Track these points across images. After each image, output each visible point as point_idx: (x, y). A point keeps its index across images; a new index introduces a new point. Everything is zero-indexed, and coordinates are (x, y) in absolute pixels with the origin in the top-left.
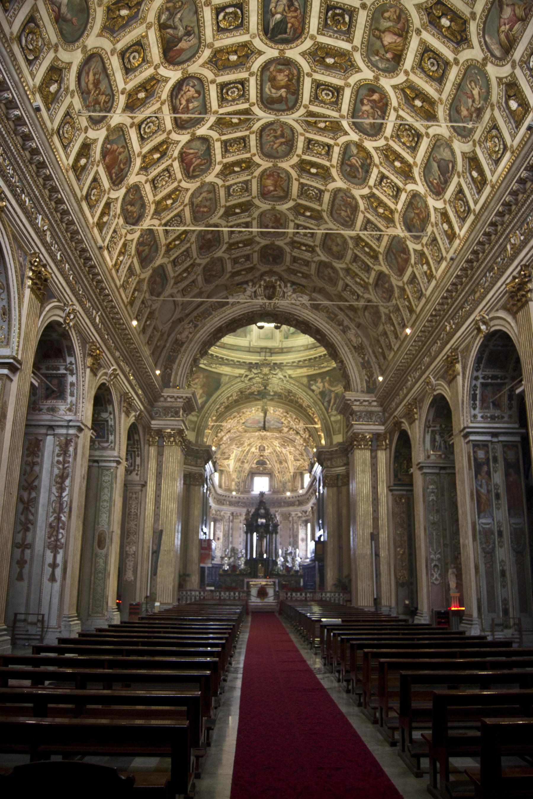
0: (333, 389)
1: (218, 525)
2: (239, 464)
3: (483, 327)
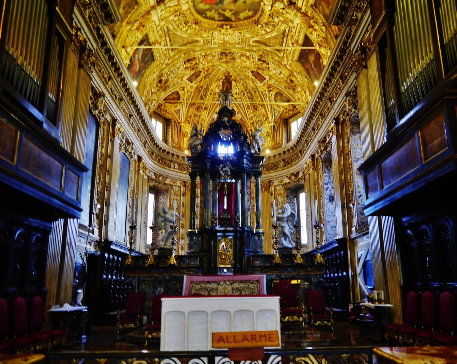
1: (162, 199)
2: (192, 111)
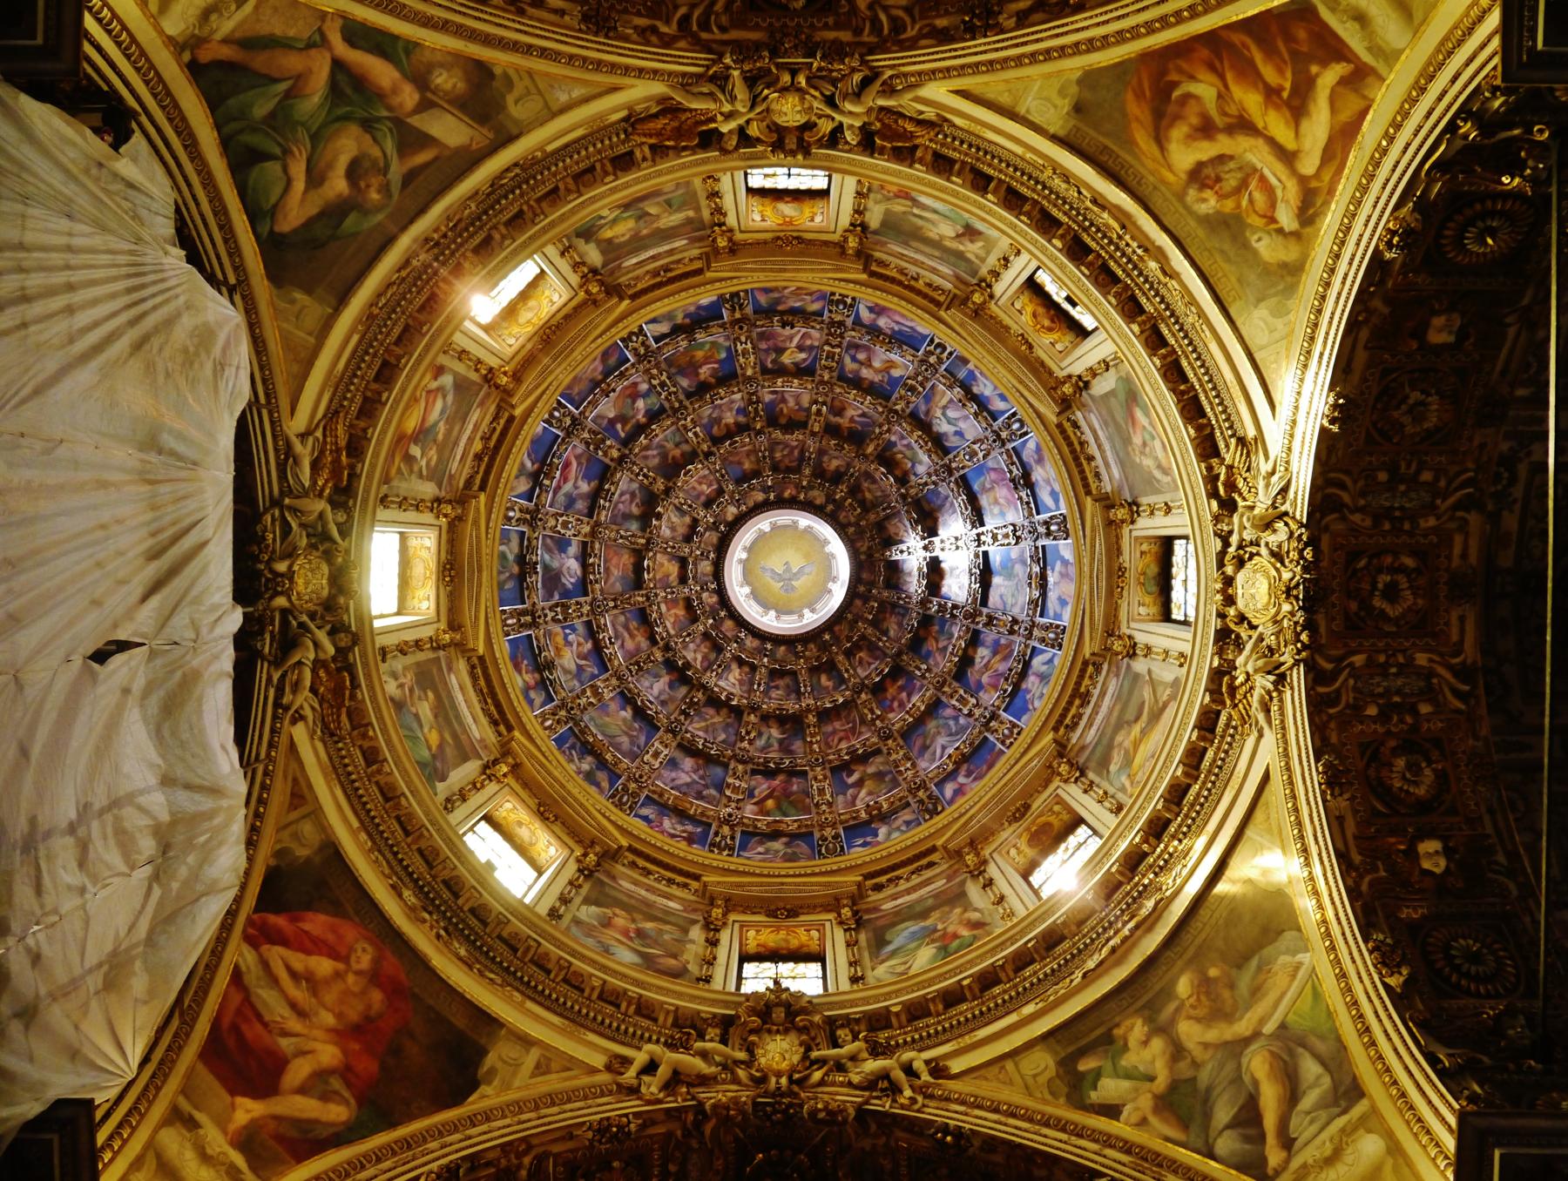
0: (1243, 1027)
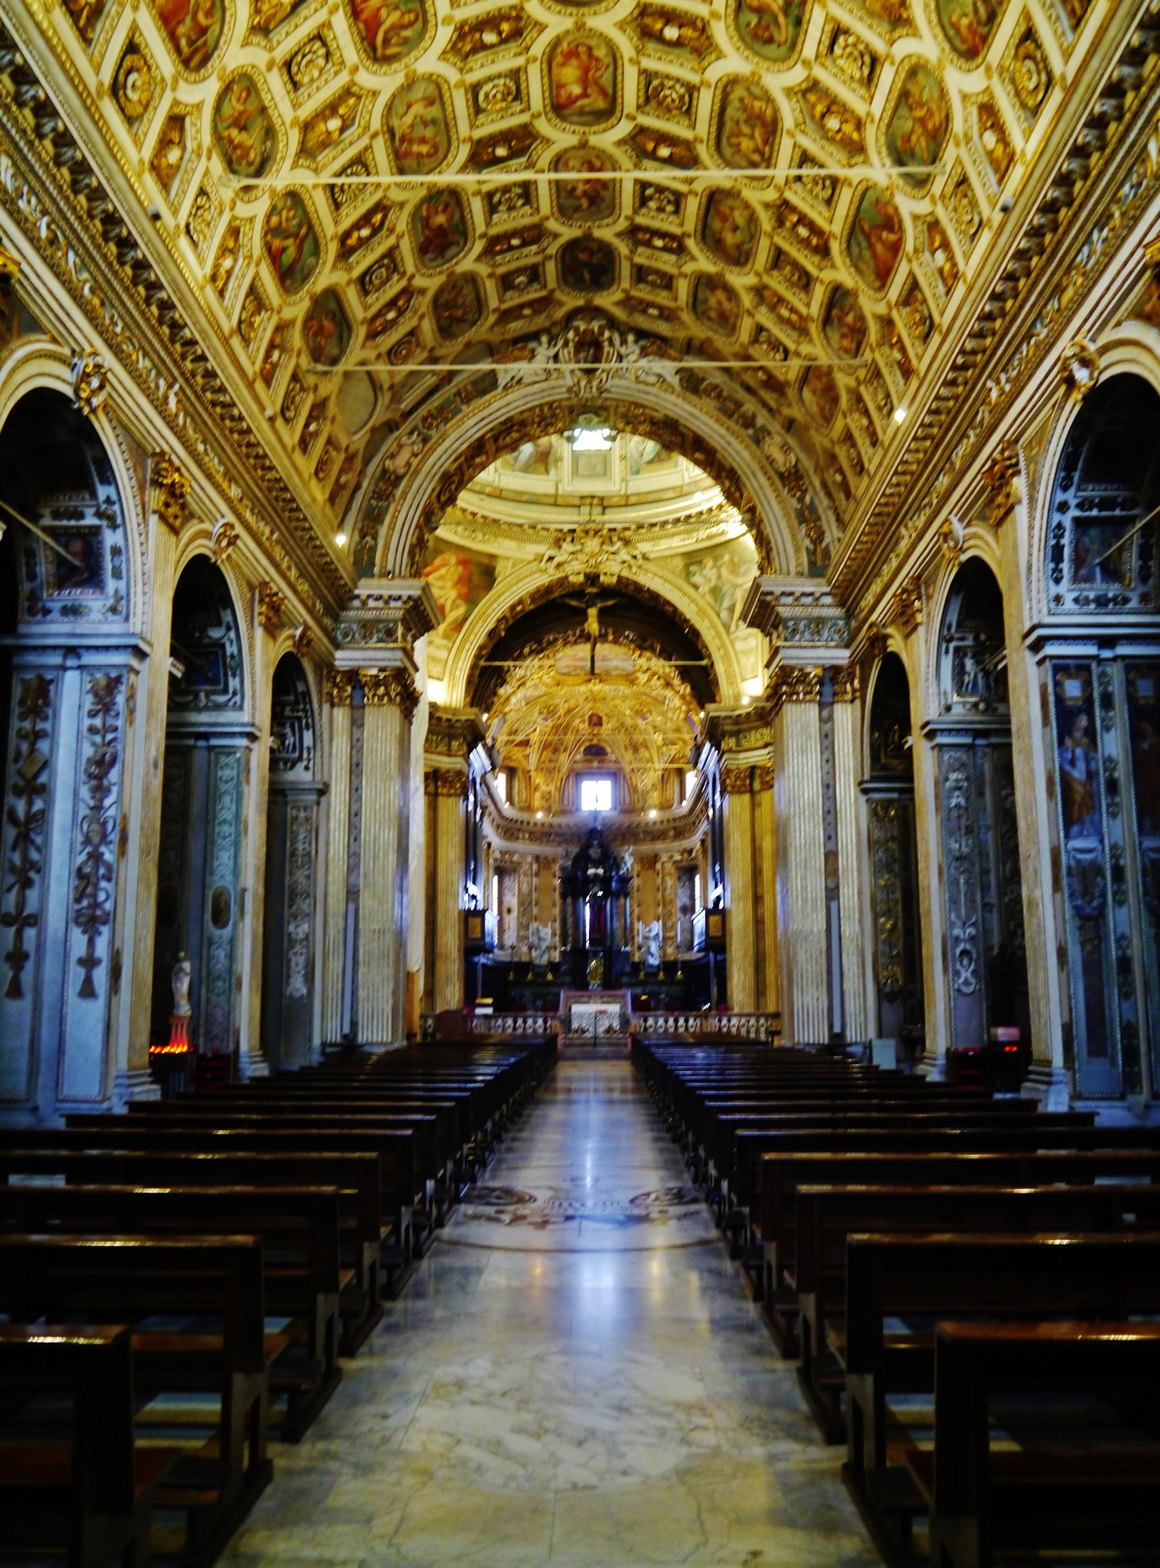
0: (739, 581)
1: (507, 882)
2: (547, 754)
3: (1082, 375)
